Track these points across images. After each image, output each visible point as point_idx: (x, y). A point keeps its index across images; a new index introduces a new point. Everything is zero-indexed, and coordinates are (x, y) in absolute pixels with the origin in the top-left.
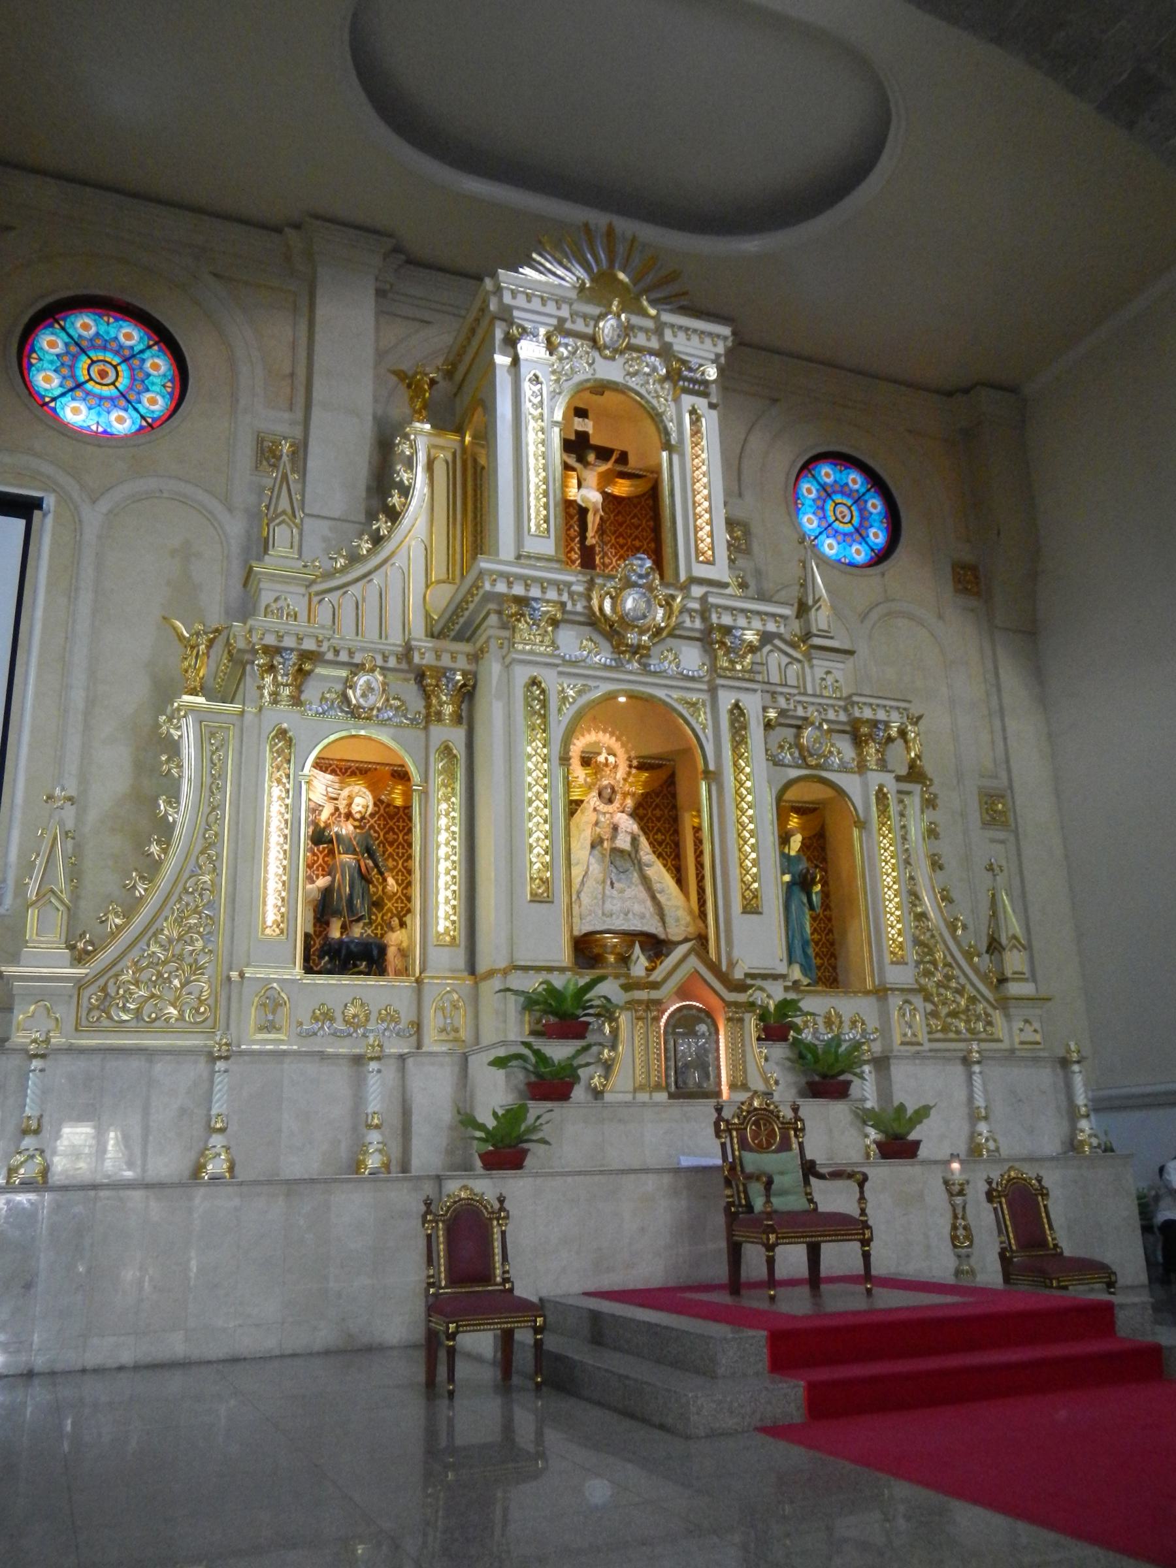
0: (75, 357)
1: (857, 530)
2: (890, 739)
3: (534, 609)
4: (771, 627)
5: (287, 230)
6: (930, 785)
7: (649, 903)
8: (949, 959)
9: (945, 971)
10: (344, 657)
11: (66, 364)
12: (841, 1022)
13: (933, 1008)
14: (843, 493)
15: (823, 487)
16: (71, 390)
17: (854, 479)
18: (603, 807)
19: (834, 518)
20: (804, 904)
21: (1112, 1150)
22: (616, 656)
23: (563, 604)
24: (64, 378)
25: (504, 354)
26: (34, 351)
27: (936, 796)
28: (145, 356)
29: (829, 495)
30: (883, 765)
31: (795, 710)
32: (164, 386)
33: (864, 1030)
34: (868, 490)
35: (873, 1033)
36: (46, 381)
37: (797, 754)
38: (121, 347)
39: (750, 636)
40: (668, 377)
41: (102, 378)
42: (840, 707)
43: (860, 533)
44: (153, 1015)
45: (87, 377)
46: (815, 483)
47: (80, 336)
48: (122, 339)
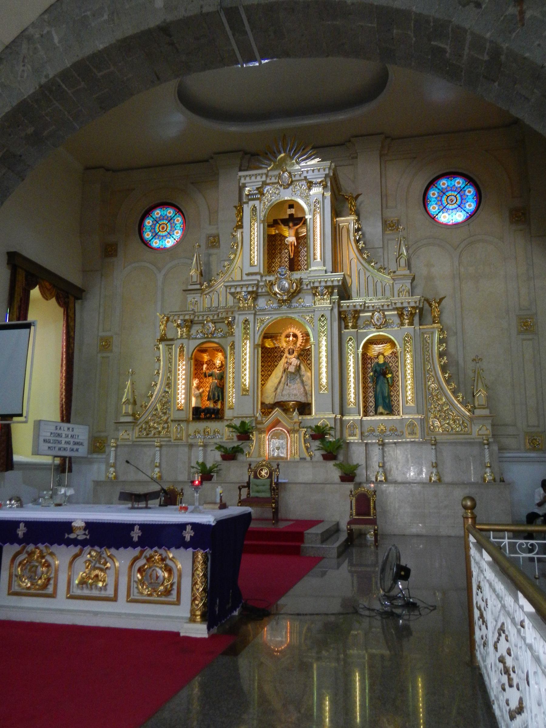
0: (155, 225)
5: (210, 160)
7: (302, 390)
10: (201, 318)
14: (452, 190)
16: (155, 236)
17: (459, 182)
18: (289, 356)
19: (447, 203)
20: (385, 383)
21: (503, 481)
28: (174, 218)
29: (444, 193)
34: (466, 185)
36: (148, 235)
41: (163, 229)
46: (437, 190)
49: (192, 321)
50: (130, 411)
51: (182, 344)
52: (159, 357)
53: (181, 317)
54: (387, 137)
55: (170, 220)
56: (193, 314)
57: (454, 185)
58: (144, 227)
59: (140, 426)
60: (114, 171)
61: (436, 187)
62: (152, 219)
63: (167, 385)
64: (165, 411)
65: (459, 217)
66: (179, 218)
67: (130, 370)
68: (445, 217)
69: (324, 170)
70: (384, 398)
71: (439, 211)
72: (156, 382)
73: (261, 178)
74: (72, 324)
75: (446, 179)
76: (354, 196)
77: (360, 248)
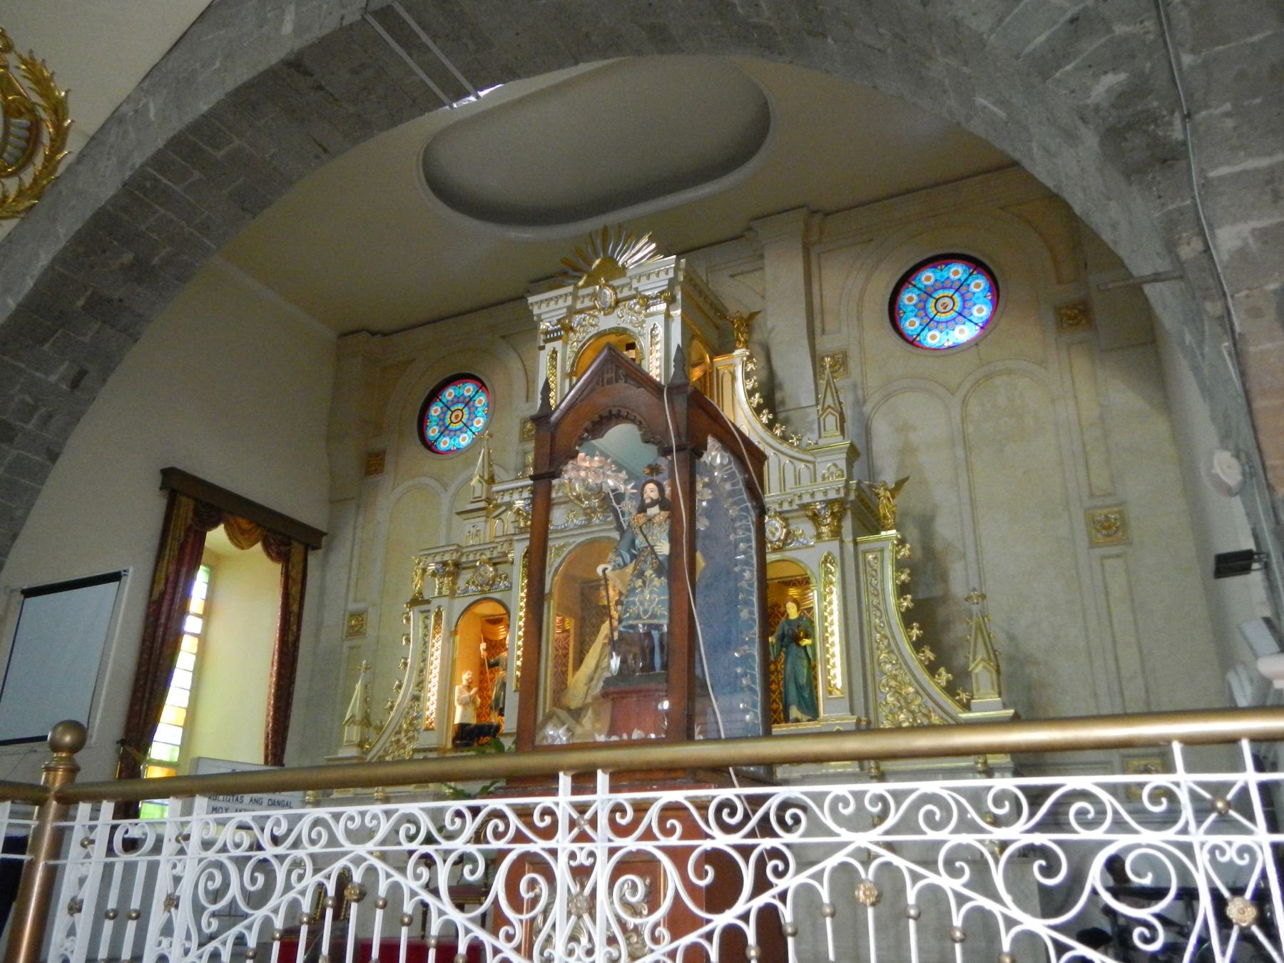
0: (445, 414)
10: (471, 558)
14: (944, 288)
17: (957, 271)
19: (935, 312)
20: (800, 658)
34: (971, 274)
36: (432, 432)
47: (448, 401)
49: (457, 565)
50: (356, 738)
51: (439, 607)
52: (409, 635)
53: (438, 559)
54: (814, 212)
55: (468, 402)
56: (457, 551)
57: (948, 278)
58: (428, 418)
60: (384, 335)
61: (914, 286)
62: (441, 405)
63: (418, 685)
64: (411, 734)
65: (964, 333)
66: (481, 398)
67: (364, 662)
68: (933, 337)
69: (667, 274)
70: (799, 688)
71: (921, 328)
72: (400, 681)
73: (565, 301)
74: (295, 590)
75: (930, 270)
76: (746, 316)
77: (755, 405)
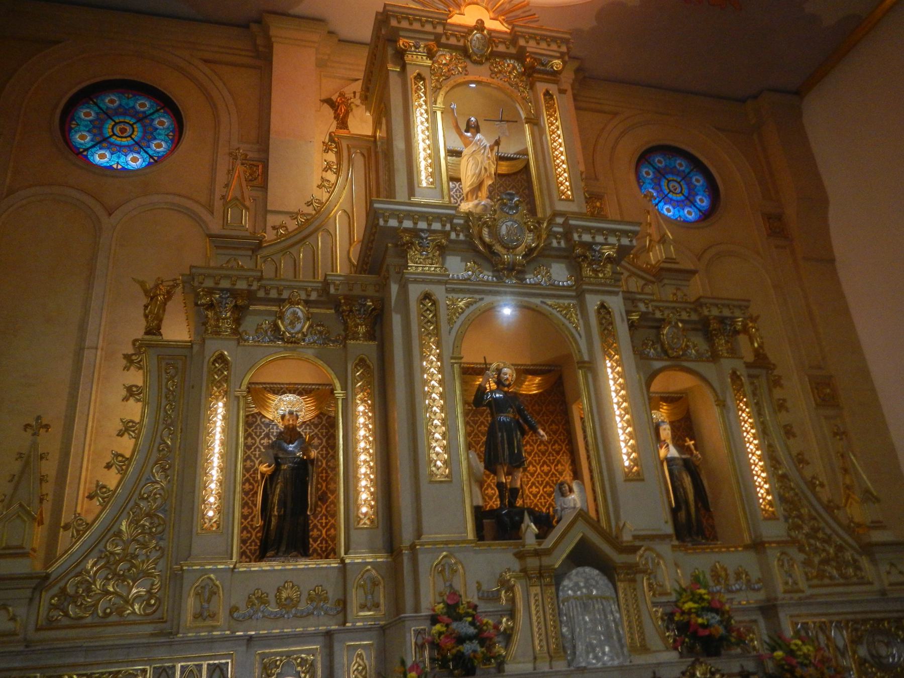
0: (103, 122)
1: (687, 198)
2: (737, 332)
3: (422, 238)
4: (625, 241)
6: (774, 369)
8: (814, 513)
9: (811, 523)
10: (273, 294)
11: (96, 128)
12: (727, 575)
13: (806, 557)
14: (672, 173)
15: (657, 170)
16: (100, 142)
17: (681, 164)
22: (496, 274)
23: (447, 234)
24: (95, 135)
25: (395, 64)
26: (74, 120)
27: (780, 377)
30: (734, 352)
31: (654, 314)
32: (167, 135)
33: (749, 581)
34: (691, 171)
35: (757, 583)
36: (82, 138)
37: (659, 349)
38: (137, 112)
39: (608, 252)
40: (523, 74)
41: (122, 133)
42: (691, 309)
43: (689, 200)
44: (108, 611)
45: (111, 133)
47: (108, 108)
48: (138, 107)
53: (225, 284)
56: (260, 279)
59: (55, 590)
